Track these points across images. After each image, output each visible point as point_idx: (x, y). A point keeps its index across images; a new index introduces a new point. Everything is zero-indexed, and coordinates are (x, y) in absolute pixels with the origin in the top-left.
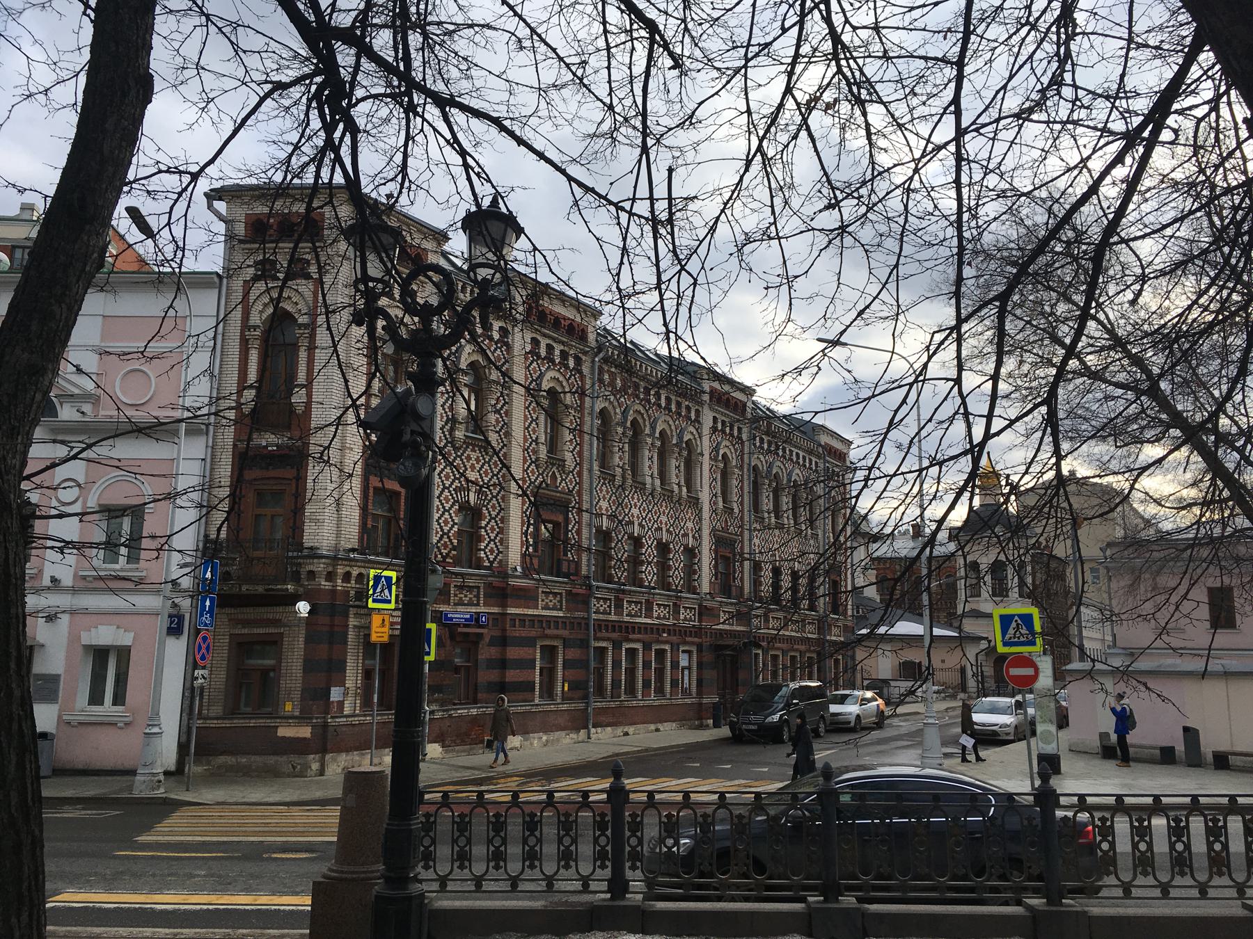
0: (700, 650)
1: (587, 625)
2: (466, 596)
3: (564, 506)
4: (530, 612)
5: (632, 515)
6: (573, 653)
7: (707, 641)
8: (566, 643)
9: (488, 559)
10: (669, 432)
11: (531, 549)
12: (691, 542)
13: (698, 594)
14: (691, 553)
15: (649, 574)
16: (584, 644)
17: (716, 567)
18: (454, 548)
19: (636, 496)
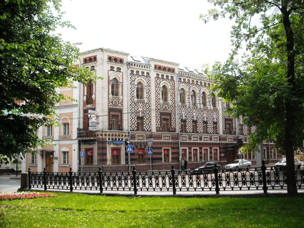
0: (220, 149)
1: (178, 143)
2: (140, 138)
3: (170, 114)
4: (160, 141)
5: (194, 115)
6: (175, 151)
7: (222, 146)
8: (172, 148)
9: (147, 129)
10: (206, 92)
11: (159, 126)
12: (215, 120)
13: (219, 134)
14: (215, 123)
15: (200, 129)
16: (178, 148)
17: (225, 126)
18: (136, 127)
19: (195, 110)
